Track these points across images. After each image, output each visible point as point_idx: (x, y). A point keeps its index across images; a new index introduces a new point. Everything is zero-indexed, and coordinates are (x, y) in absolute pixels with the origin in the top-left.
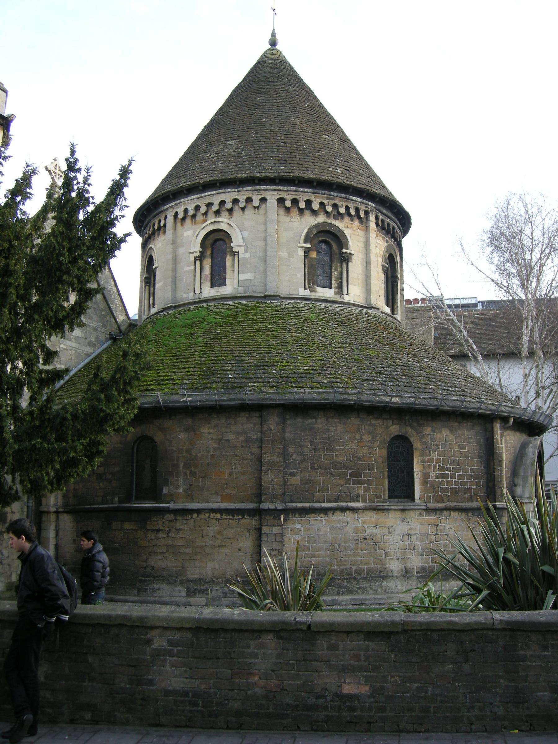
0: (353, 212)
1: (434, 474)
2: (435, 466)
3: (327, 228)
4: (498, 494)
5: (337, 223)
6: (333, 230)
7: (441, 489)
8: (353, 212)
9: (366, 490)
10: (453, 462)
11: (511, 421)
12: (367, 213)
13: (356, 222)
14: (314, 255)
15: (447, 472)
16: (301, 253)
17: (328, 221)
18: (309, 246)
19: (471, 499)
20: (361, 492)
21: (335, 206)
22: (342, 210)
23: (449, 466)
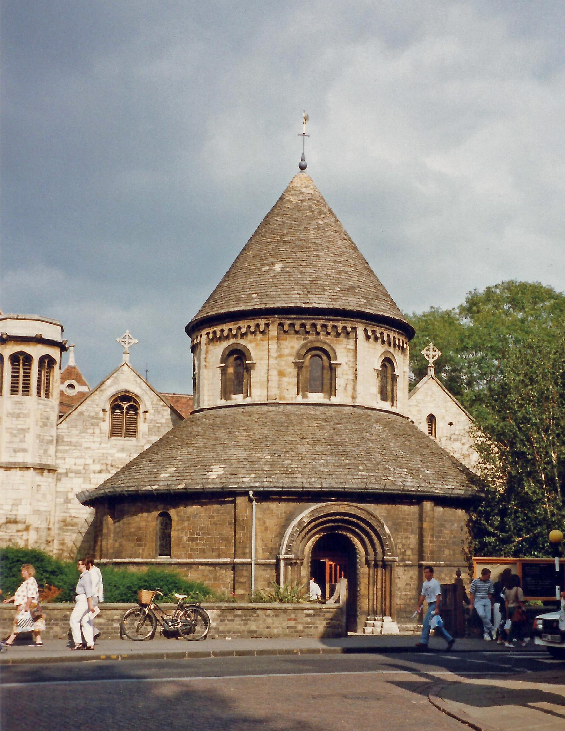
0: (252, 329)
1: (185, 539)
2: (186, 533)
3: (235, 347)
4: (239, 551)
5: (242, 342)
6: (239, 348)
7: (191, 549)
8: (252, 329)
9: (143, 550)
10: (202, 529)
11: (251, 493)
12: (267, 325)
13: (259, 336)
14: (231, 370)
15: (196, 536)
16: (219, 371)
17: (235, 342)
18: (223, 365)
19: (219, 556)
20: (141, 551)
21: (240, 328)
22: (243, 330)
23: (198, 532)
